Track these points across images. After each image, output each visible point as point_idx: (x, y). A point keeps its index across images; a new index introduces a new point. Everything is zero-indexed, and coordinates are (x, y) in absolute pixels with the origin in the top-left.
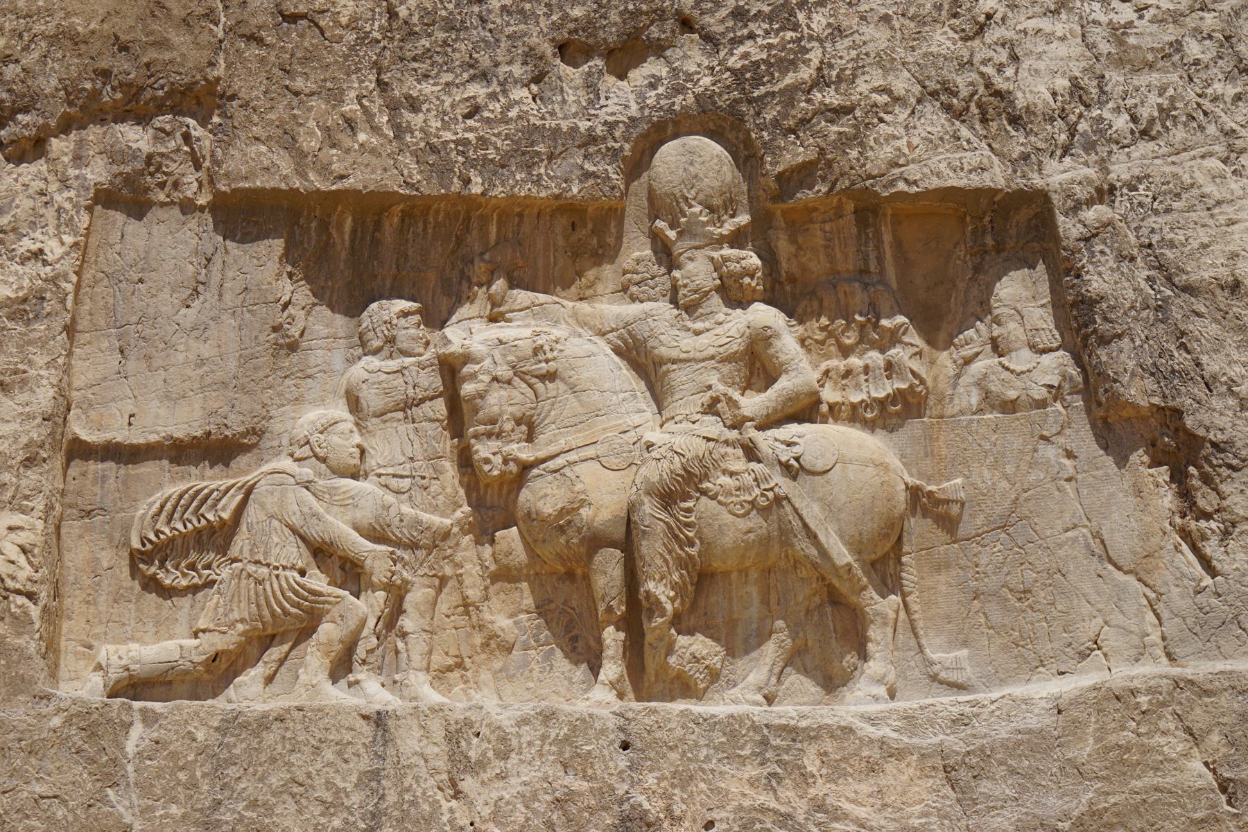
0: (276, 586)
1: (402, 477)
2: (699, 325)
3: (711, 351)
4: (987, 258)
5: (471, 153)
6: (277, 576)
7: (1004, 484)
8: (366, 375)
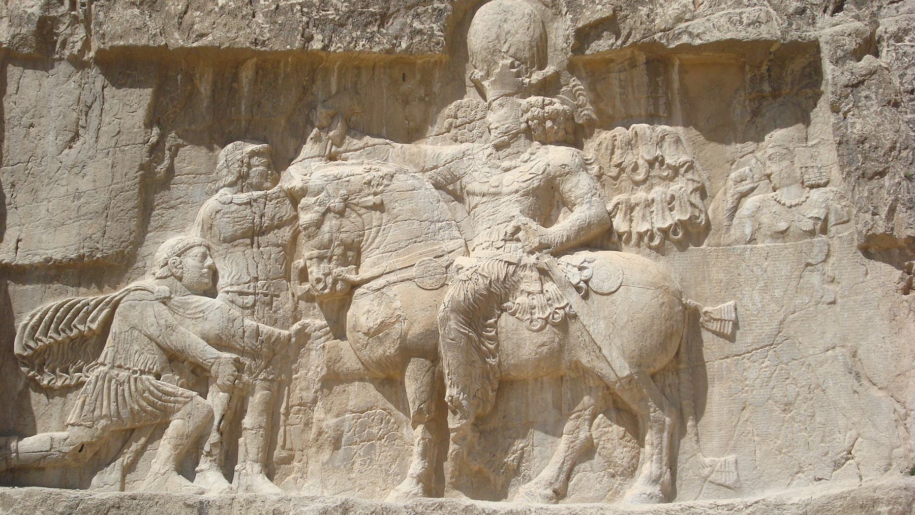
0: (133, 387)
1: (247, 294)
2: (506, 164)
3: (515, 186)
4: (765, 103)
5: (314, 13)
6: (136, 379)
7: (773, 307)
8: (219, 207)
